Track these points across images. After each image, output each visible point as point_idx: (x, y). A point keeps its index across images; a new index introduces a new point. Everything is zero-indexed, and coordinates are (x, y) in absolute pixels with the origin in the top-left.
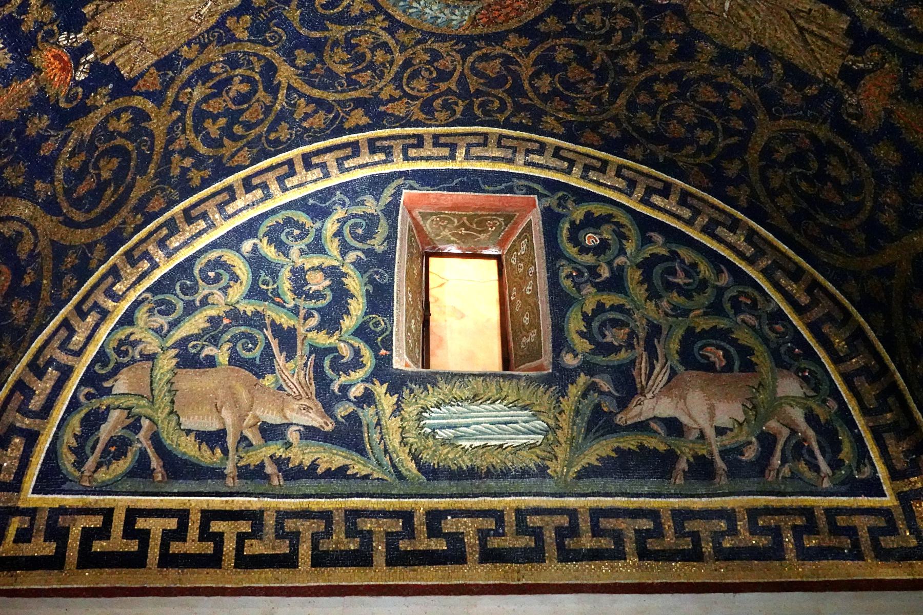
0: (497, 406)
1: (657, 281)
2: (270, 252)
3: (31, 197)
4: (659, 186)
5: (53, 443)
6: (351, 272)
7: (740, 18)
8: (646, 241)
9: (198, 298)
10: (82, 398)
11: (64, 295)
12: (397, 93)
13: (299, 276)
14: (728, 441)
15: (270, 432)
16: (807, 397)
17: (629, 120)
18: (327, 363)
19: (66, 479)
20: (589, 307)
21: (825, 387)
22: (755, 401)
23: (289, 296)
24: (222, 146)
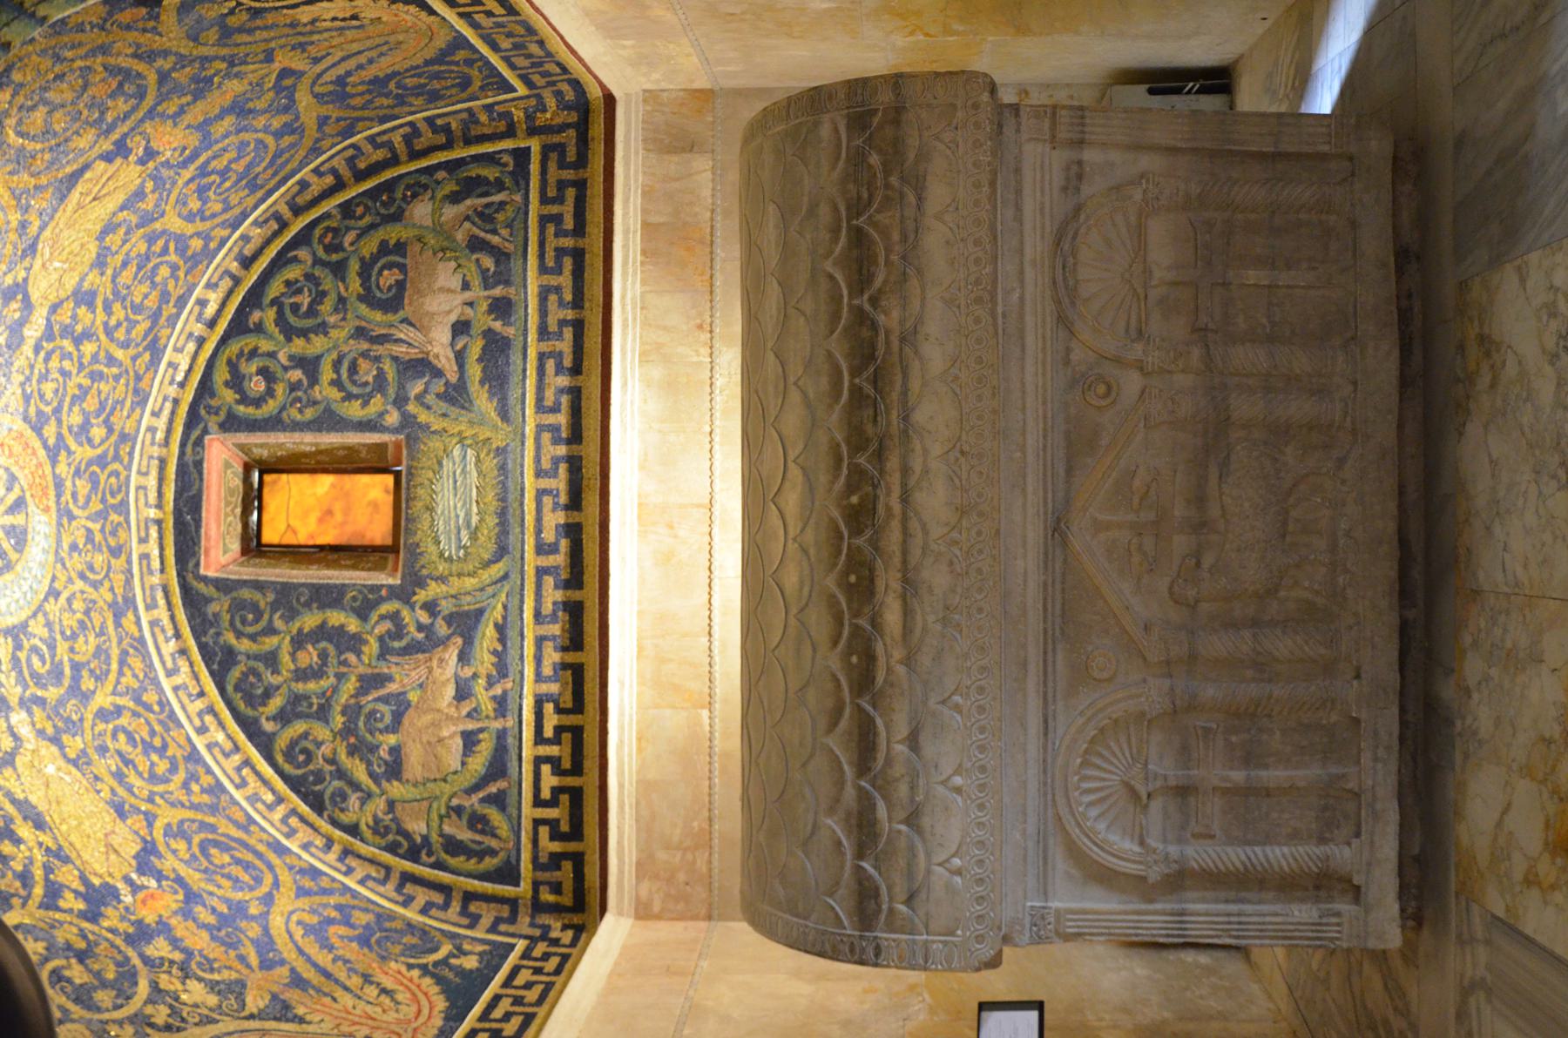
0: (437, 488)
1: (308, 323)
2: (276, 703)
3: (265, 915)
4: (197, 308)
5: (475, 877)
6: (298, 625)
7: (71, 253)
8: (259, 328)
9: (328, 768)
10: (433, 859)
11: (336, 885)
12: (107, 584)
13: (302, 675)
14: (476, 282)
15: (463, 693)
16: (432, 198)
17: (137, 345)
18: (396, 644)
19: (508, 862)
20: (335, 394)
21: (424, 179)
22: (437, 247)
23: (325, 683)
24: (174, 757)
